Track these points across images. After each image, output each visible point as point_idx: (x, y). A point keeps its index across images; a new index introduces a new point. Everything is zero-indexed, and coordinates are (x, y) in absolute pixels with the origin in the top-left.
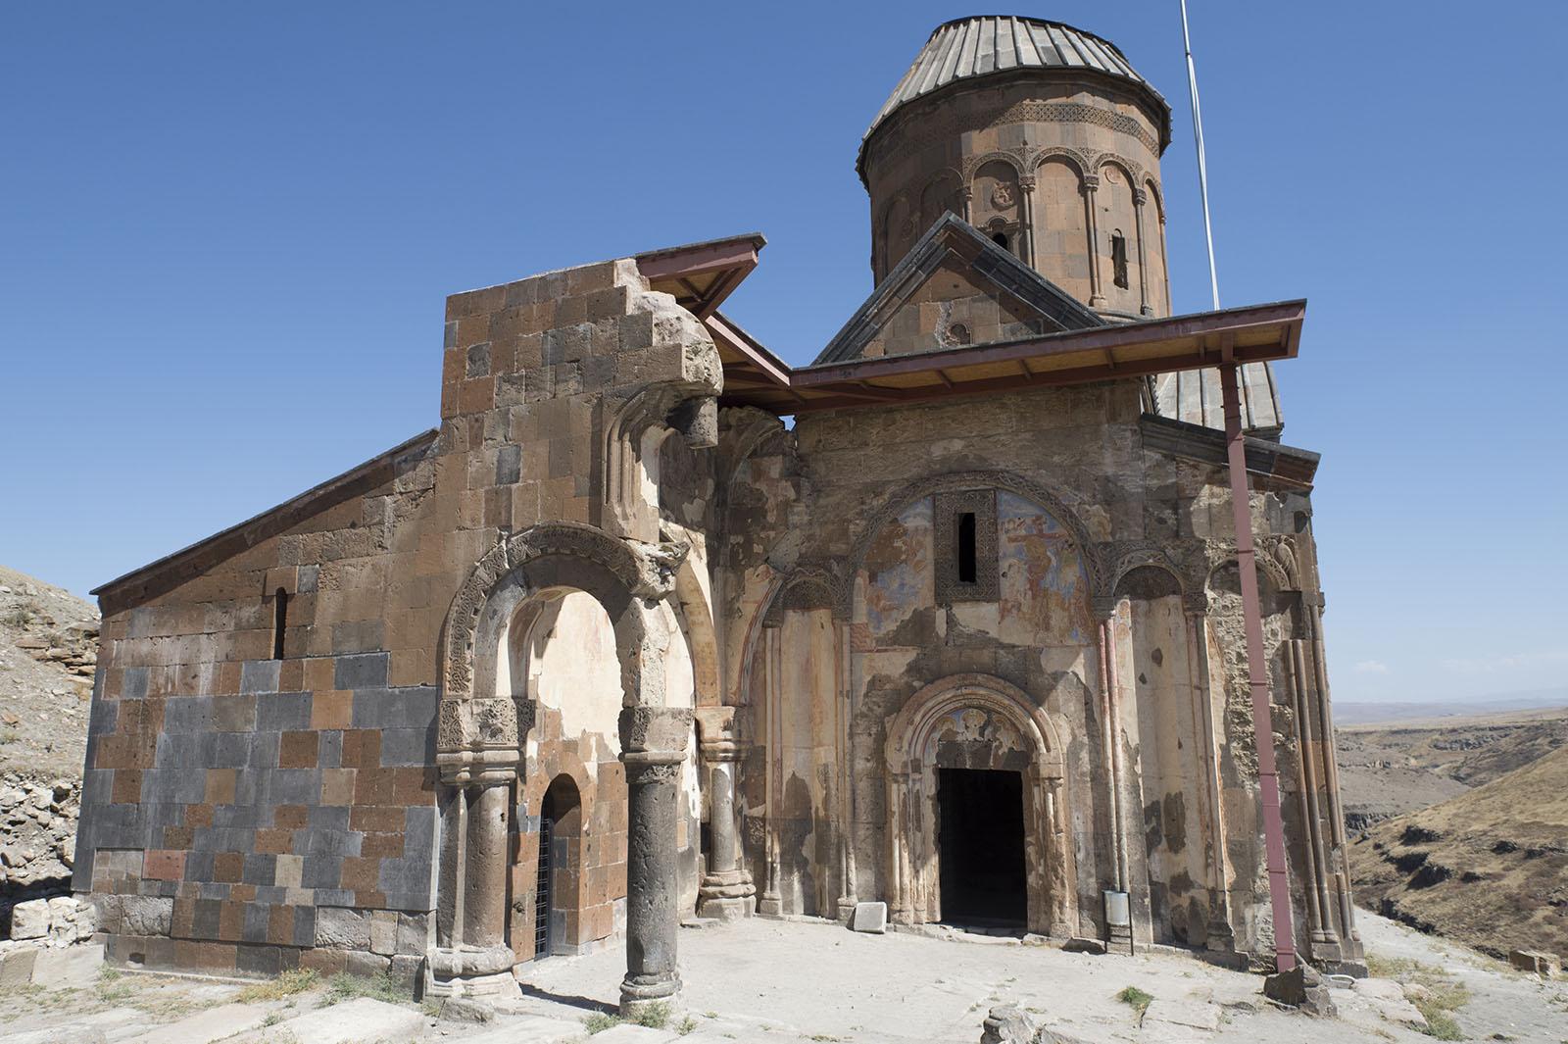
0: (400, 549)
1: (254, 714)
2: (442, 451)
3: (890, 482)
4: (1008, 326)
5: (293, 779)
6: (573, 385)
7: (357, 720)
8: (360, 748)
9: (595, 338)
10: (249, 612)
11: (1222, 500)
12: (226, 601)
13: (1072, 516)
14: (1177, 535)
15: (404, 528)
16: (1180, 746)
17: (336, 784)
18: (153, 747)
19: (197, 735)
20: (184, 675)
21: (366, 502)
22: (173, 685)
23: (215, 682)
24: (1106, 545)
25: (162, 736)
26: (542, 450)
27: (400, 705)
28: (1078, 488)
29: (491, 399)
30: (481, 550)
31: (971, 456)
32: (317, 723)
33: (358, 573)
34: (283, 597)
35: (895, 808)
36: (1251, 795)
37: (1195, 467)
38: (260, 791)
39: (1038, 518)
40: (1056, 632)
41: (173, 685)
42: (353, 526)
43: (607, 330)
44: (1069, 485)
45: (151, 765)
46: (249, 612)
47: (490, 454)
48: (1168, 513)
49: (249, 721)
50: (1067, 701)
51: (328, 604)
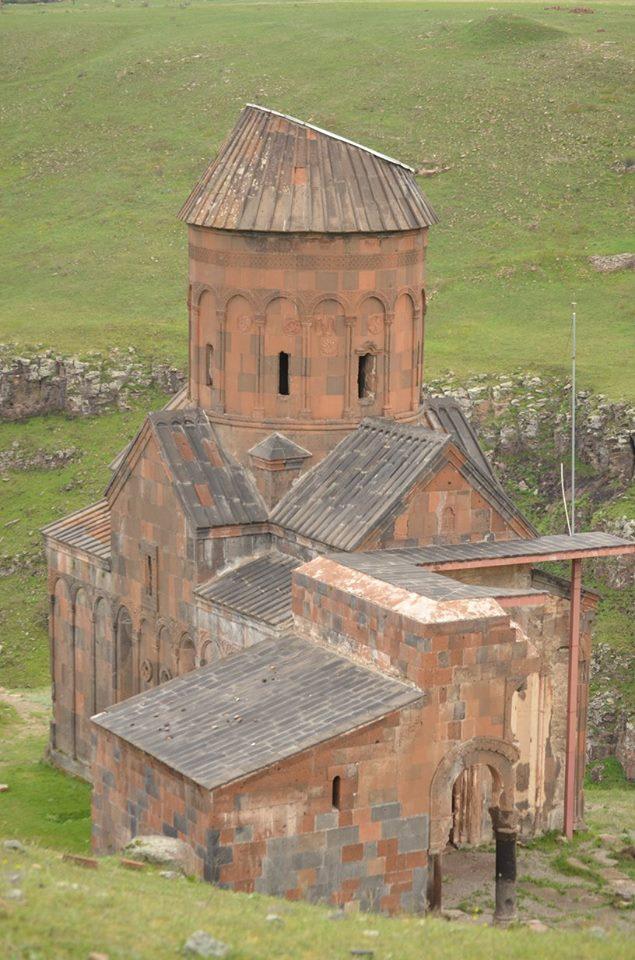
0: (404, 752)
1: (325, 840)
2: (425, 704)
4: (474, 511)
5: (354, 866)
7: (385, 835)
8: (387, 848)
9: (501, 652)
10: (316, 790)
12: (300, 785)
14: (541, 633)
15: (406, 743)
17: (374, 865)
18: (260, 865)
19: (289, 854)
20: (277, 828)
21: (386, 730)
22: (270, 833)
23: (298, 828)
25: (266, 859)
26: (476, 704)
27: (407, 825)
29: (451, 679)
30: (445, 751)
32: (362, 840)
33: (381, 765)
34: (337, 780)
37: (552, 598)
38: (331, 875)
41: (270, 833)
42: (377, 742)
43: (507, 648)
45: (260, 875)
46: (316, 790)
47: (450, 705)
49: (321, 844)
51: (365, 782)
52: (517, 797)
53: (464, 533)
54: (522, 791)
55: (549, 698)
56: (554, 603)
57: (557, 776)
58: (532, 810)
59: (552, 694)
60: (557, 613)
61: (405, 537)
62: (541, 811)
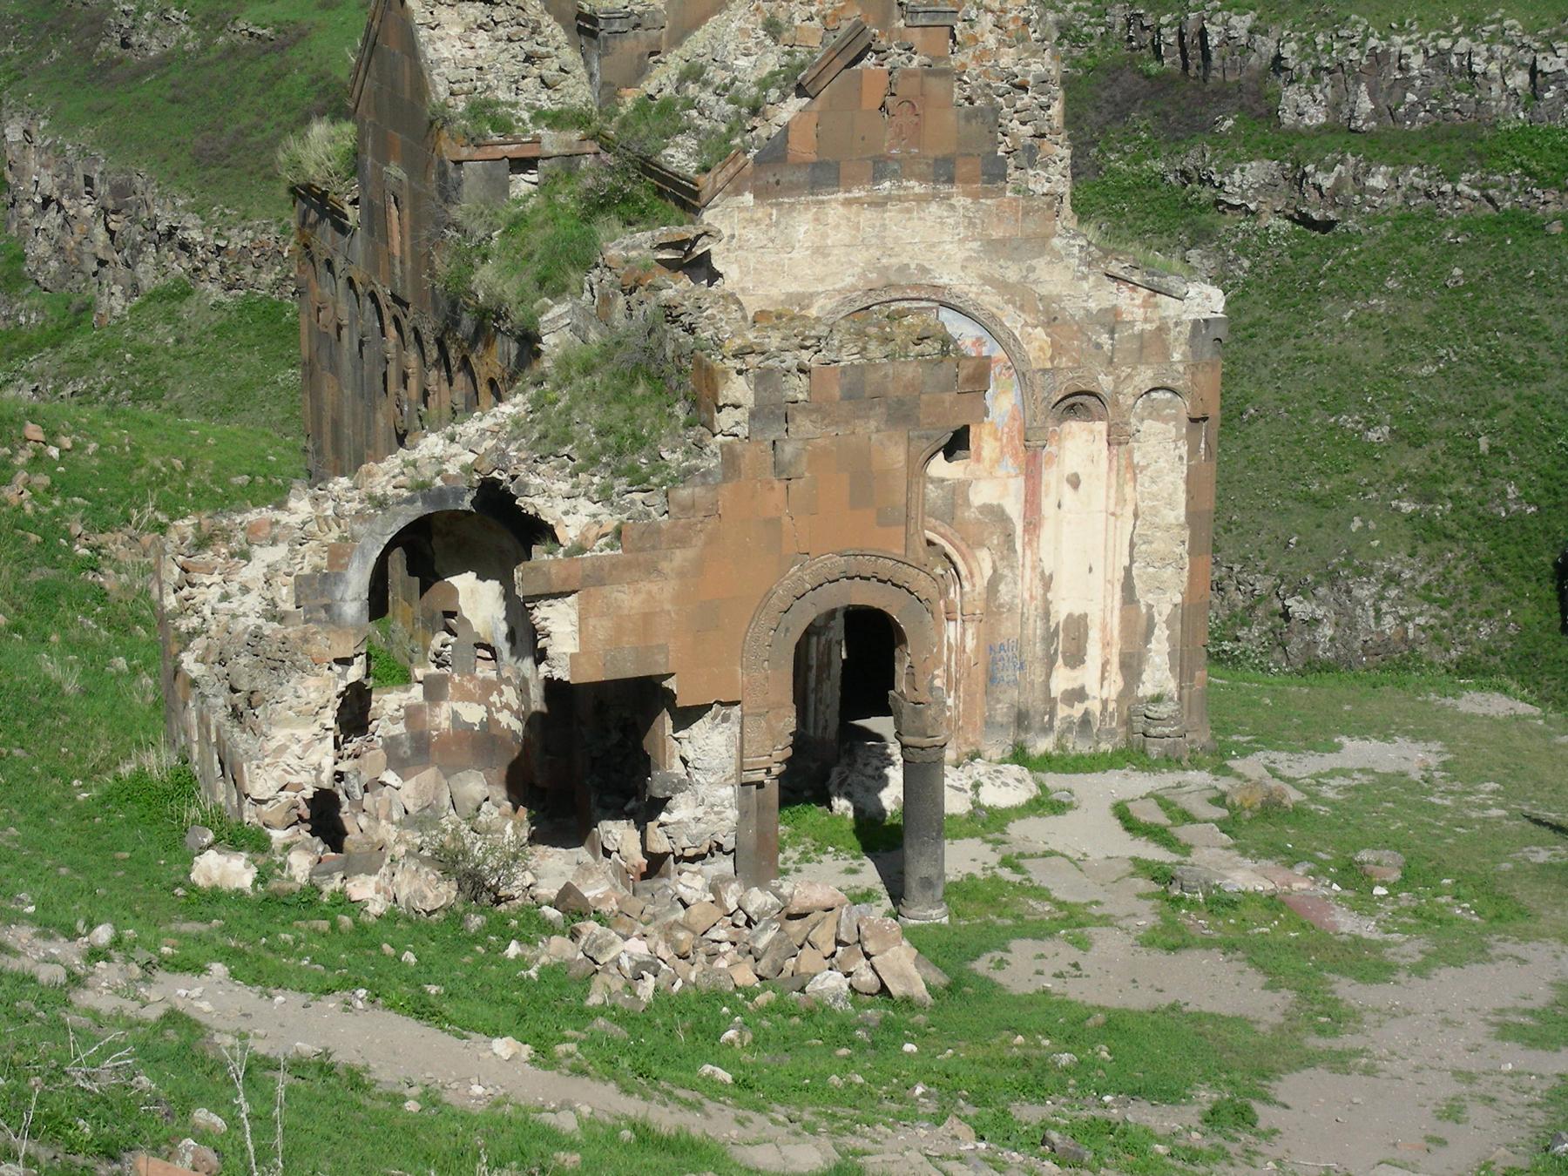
3: (819, 294)
6: (873, 424)
11: (1154, 326)
13: (1015, 339)
14: (1111, 362)
16: (1091, 570)
24: (1045, 371)
28: (1022, 308)
31: (913, 266)
35: (814, 662)
36: (1144, 610)
39: (979, 339)
40: (987, 463)
44: (1014, 304)
48: (1104, 338)
50: (992, 534)
52: (1062, 680)
53: (939, 153)
54: (1073, 667)
55: (1128, 489)
56: (1138, 302)
57: (1147, 640)
58: (1095, 706)
59: (1135, 481)
60: (1146, 320)
61: (814, 158)
62: (1112, 706)
